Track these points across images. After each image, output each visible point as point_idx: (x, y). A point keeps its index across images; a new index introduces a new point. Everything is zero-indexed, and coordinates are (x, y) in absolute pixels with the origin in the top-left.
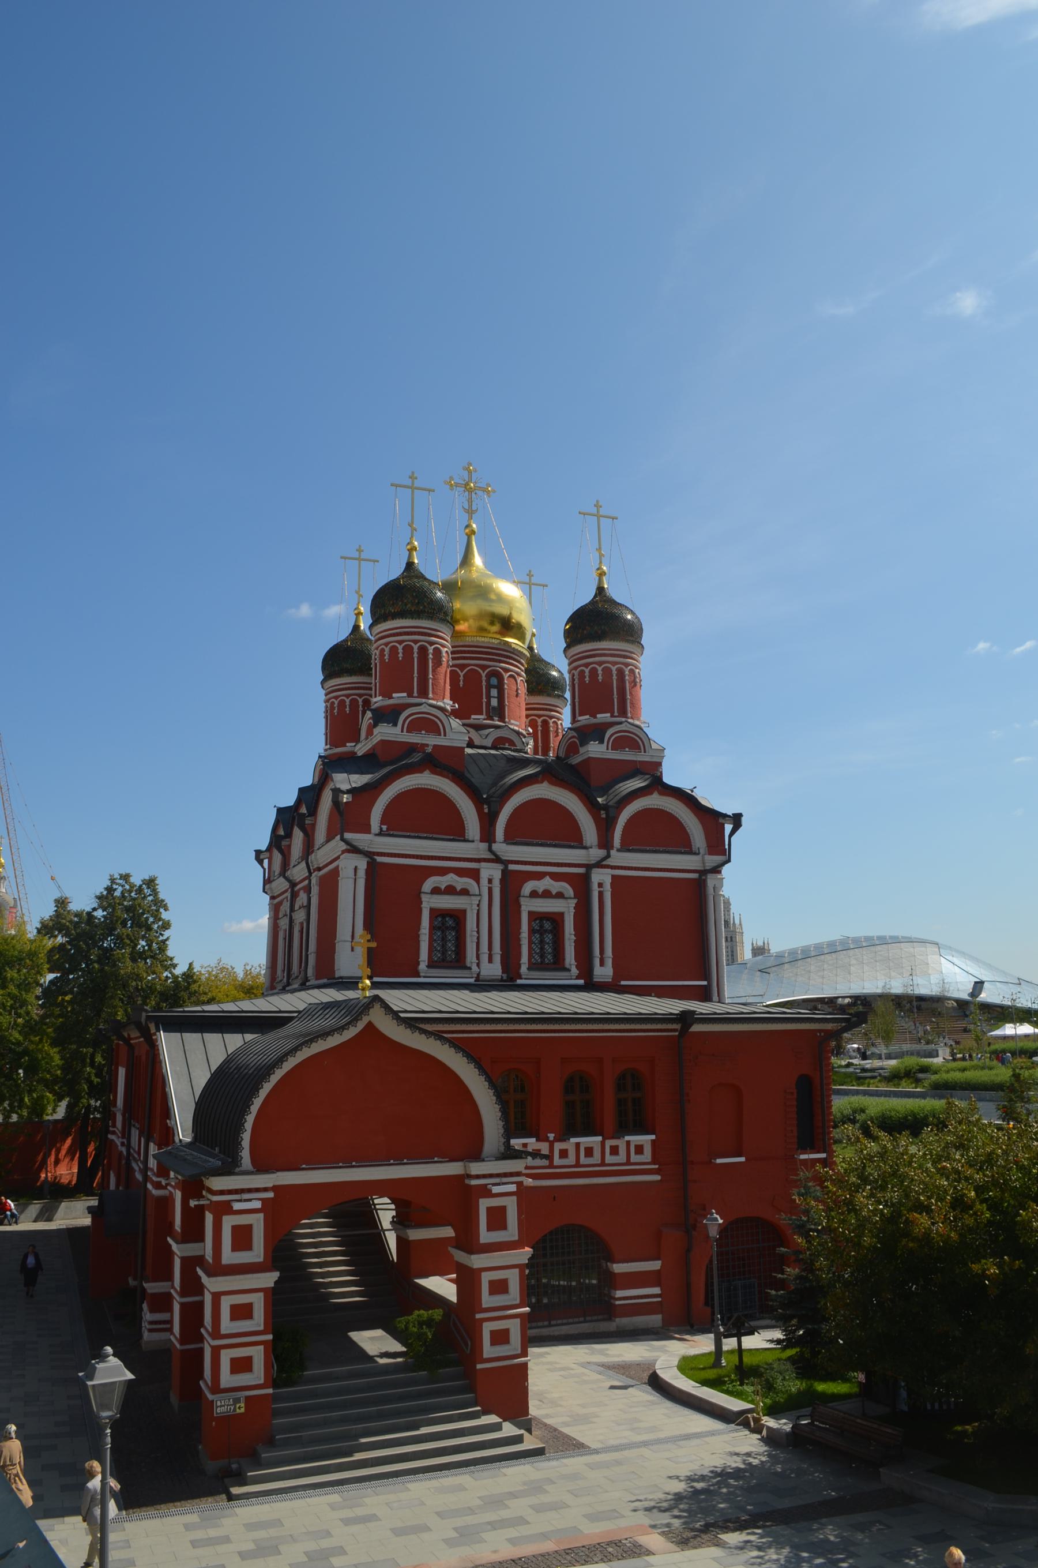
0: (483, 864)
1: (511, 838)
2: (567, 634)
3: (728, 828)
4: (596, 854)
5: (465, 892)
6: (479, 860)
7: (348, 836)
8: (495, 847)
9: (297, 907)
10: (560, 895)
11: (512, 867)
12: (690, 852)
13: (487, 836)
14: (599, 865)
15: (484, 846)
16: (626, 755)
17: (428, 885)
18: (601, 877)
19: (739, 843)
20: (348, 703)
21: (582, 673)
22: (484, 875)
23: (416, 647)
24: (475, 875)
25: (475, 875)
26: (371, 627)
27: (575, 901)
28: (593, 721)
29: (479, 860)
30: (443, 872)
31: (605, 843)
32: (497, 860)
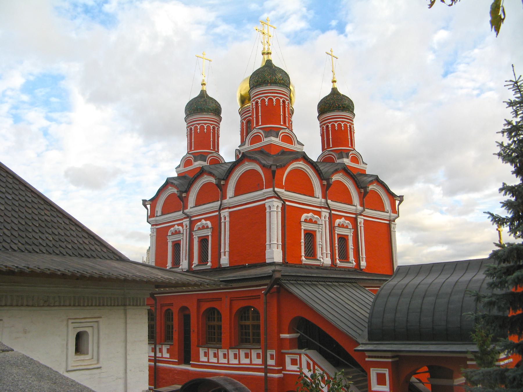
0: (323, 210)
3: (397, 202)
5: (315, 222)
7: (276, 189)
10: (347, 227)
11: (333, 212)
12: (383, 211)
17: (304, 216)
18: (361, 220)
19: (402, 208)
20: (199, 128)
22: (323, 214)
24: (319, 214)
25: (319, 214)
27: (353, 230)
29: (320, 207)
30: (308, 211)
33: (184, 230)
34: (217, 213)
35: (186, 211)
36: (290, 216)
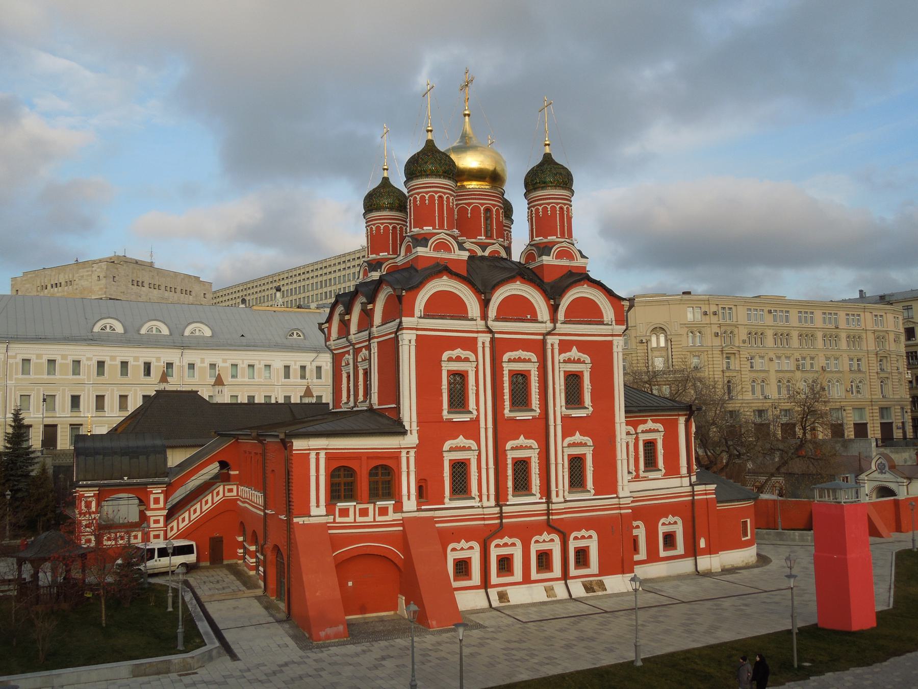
1: (497, 319)
2: (526, 185)
4: (550, 326)
6: (478, 332)
8: (490, 323)
9: (359, 360)
13: (484, 317)
14: (549, 333)
15: (483, 322)
16: (564, 262)
21: (537, 210)
23: (436, 196)
26: (405, 183)
28: (545, 240)
29: (478, 332)
31: (554, 320)
32: (490, 331)
33: (350, 358)
34: (393, 335)
35: (350, 337)
36: (430, 349)
